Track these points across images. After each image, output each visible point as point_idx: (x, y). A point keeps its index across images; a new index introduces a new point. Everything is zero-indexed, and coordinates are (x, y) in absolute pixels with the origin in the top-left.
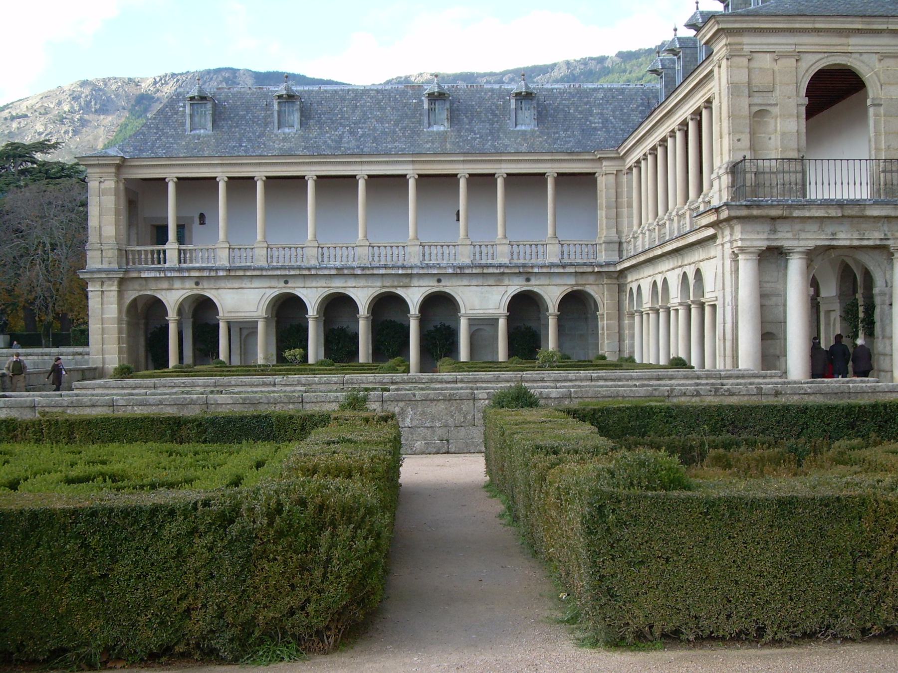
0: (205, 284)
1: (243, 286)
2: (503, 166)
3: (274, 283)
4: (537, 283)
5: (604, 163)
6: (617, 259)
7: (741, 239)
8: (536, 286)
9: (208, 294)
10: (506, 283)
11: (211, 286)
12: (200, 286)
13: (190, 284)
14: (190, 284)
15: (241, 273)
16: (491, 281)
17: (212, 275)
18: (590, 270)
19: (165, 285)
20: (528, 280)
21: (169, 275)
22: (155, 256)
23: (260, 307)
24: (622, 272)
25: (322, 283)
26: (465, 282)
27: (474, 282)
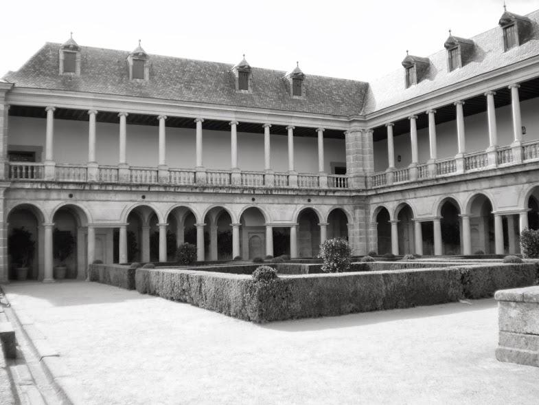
0: (77, 196)
3: (134, 197)
4: (315, 203)
6: (364, 188)
10: (296, 202)
11: (83, 198)
13: (65, 195)
14: (65, 195)
16: (287, 200)
17: (85, 187)
18: (348, 194)
24: (367, 196)
25: (170, 198)
26: (270, 201)
27: (276, 201)
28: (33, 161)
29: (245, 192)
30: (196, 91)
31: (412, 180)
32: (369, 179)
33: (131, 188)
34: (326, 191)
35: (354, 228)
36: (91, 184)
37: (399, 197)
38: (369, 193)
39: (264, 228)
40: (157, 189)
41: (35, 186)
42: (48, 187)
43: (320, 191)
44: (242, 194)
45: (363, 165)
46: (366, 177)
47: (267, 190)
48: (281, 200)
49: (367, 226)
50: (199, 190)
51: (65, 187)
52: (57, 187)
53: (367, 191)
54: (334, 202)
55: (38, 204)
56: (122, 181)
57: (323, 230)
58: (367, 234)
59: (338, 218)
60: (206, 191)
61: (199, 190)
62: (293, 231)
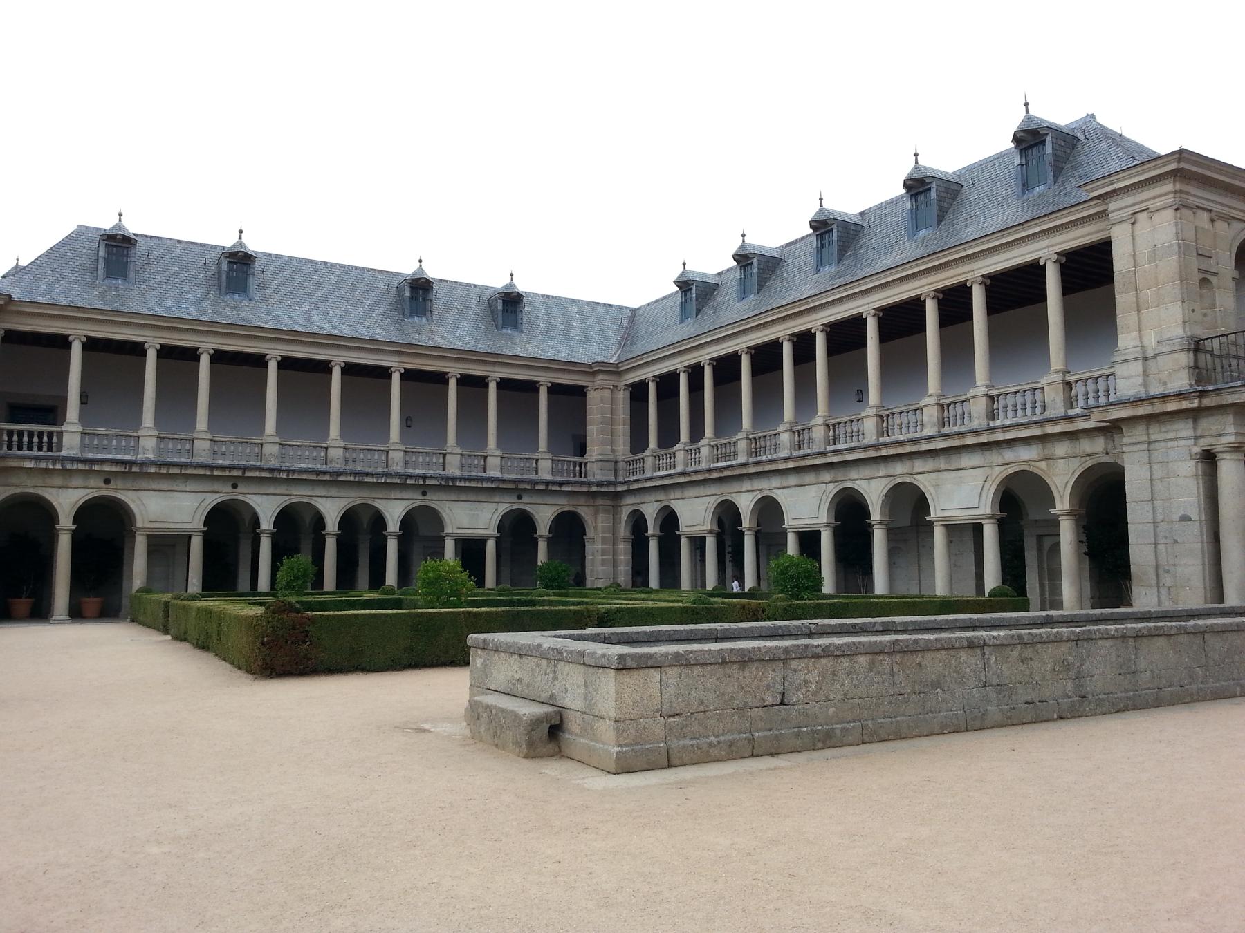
0: (119, 483)
1: (175, 488)
2: (497, 369)
5: (601, 377)
6: (612, 479)
7: (1236, 434)
8: (528, 504)
9: (121, 495)
11: (128, 486)
12: (112, 485)
13: (97, 482)
15: (176, 471)
17: (135, 472)
18: (585, 489)
19: (58, 481)
20: (520, 497)
21: (69, 467)
22: (45, 439)
23: (197, 516)
27: (463, 497)
28: (54, 423)
29: (409, 482)
30: (335, 315)
31: (679, 469)
32: (621, 465)
33: (209, 474)
34: (547, 483)
35: (595, 549)
36: (142, 464)
37: (661, 496)
38: (619, 489)
39: (441, 540)
40: (257, 474)
41: (43, 465)
42: (67, 471)
43: (536, 483)
44: (403, 486)
45: (612, 443)
46: (616, 462)
47: (447, 478)
48: (472, 497)
49: (614, 543)
50: (332, 480)
51: (97, 468)
52: (81, 467)
53: (615, 484)
54: (563, 501)
55: (51, 495)
56: (197, 460)
57: (542, 546)
58: (615, 553)
59: (569, 531)
60: (340, 479)
61: (332, 480)
62: (491, 546)
